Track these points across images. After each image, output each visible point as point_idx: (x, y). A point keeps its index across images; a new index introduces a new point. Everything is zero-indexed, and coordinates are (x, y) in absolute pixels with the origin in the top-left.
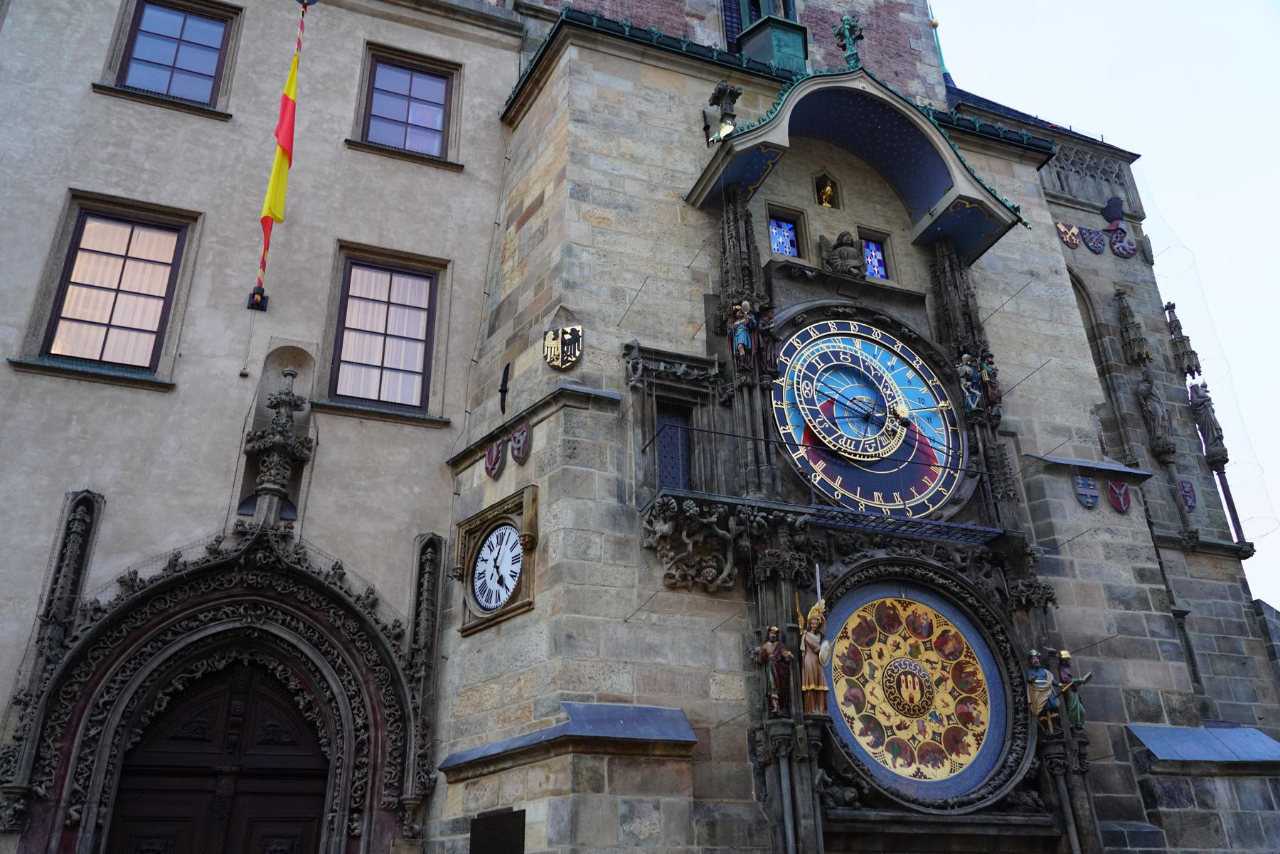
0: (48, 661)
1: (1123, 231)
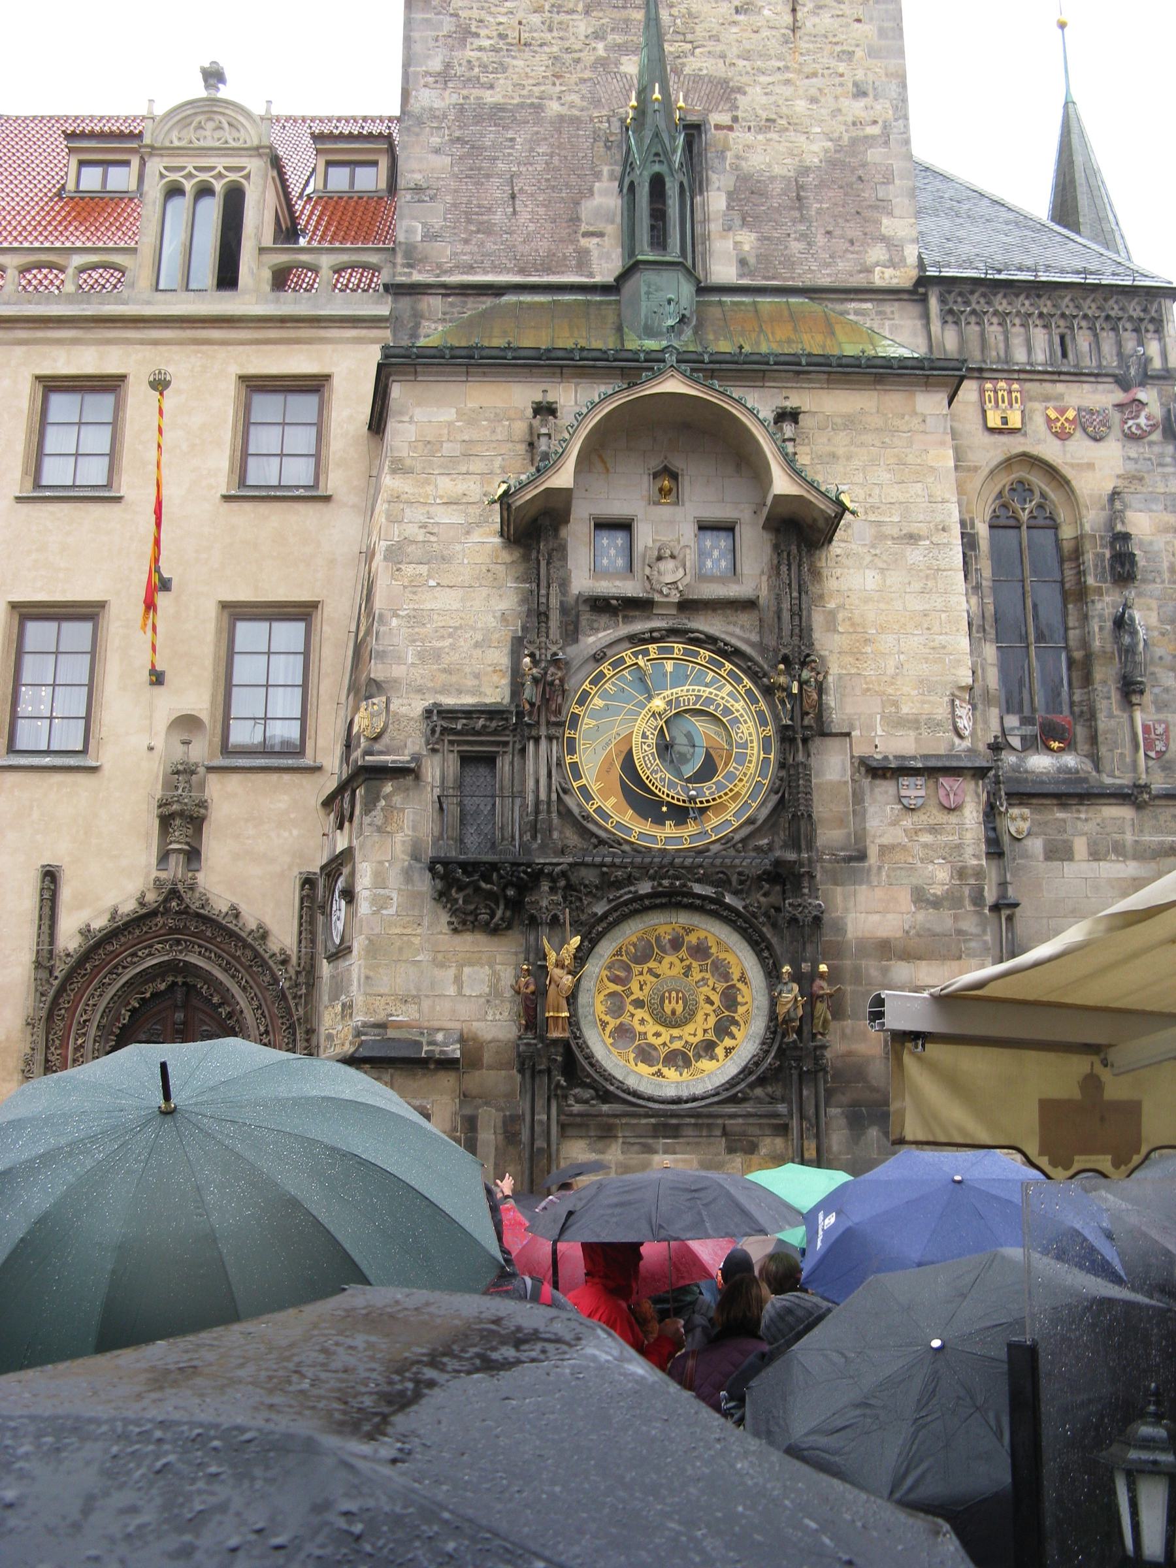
0: (42, 995)
1: (1139, 401)
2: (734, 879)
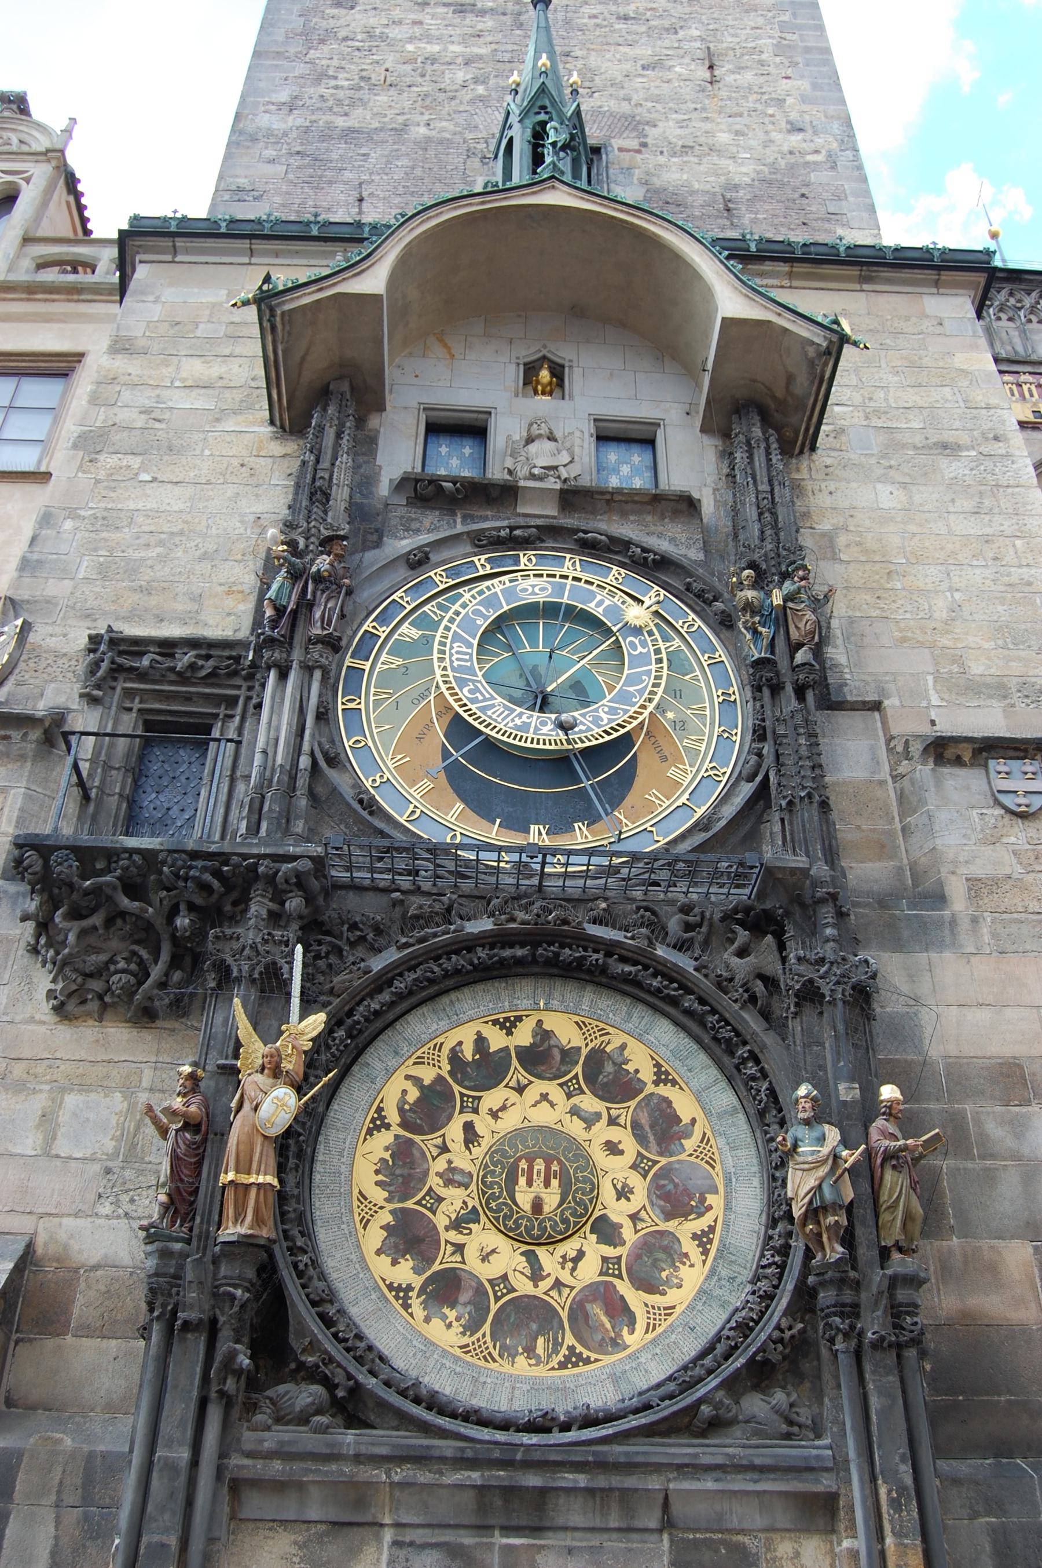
2: (674, 924)
